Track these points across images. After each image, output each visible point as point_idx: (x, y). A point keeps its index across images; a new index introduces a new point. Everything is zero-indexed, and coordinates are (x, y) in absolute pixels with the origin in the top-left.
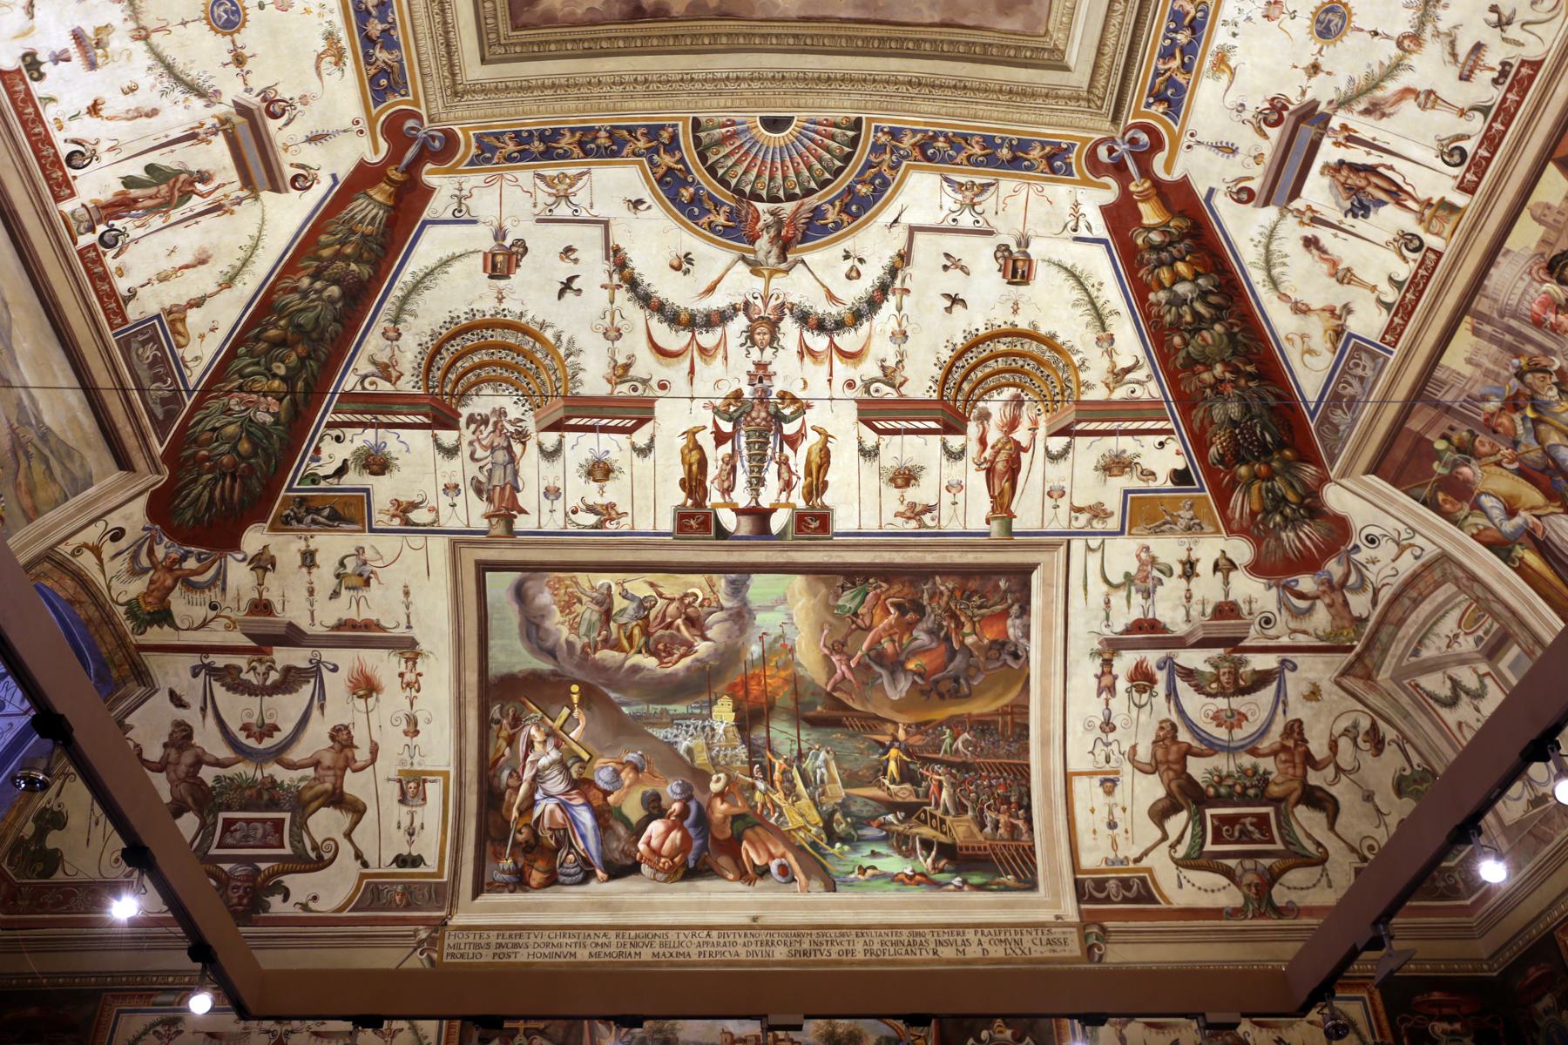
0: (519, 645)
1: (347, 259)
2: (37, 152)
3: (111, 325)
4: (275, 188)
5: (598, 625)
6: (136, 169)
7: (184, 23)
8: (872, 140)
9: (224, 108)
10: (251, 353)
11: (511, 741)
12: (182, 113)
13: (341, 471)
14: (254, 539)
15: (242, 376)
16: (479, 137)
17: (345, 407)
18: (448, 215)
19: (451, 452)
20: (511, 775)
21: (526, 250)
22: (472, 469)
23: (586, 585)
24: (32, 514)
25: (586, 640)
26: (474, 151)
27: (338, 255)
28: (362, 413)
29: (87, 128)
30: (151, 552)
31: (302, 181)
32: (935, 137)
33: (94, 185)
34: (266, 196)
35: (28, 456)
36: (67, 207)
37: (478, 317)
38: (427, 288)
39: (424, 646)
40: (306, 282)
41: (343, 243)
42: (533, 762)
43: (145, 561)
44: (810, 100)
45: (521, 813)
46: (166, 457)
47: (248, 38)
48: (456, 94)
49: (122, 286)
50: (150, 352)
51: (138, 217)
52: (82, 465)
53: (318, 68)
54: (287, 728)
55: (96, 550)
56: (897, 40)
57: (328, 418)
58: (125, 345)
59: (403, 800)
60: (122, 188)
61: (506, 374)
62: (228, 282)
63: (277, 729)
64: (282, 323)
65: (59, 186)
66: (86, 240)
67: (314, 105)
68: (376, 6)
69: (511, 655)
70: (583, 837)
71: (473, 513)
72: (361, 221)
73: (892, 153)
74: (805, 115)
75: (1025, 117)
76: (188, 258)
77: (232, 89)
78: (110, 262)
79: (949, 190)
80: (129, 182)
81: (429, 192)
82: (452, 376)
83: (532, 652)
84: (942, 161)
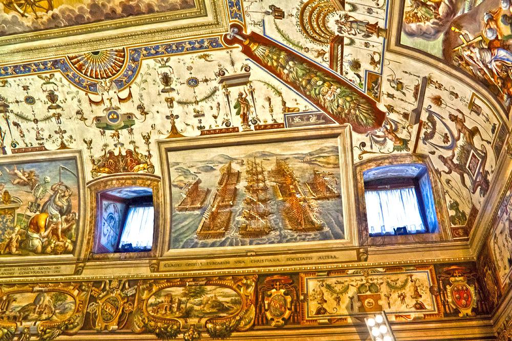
0: (432, 43)
1: (278, 59)
2: (223, 133)
3: (282, 128)
4: (249, 76)
5: (427, 9)
6: (234, 111)
7: (195, 92)
9: (220, 87)
10: (310, 91)
11: (467, 64)
12: (220, 97)
13: (359, 76)
14: (381, 107)
15: (319, 94)
16: (232, 18)
17: (335, 68)
18: (262, 28)
19: (352, 42)
20: (480, 72)
21: (273, 5)
22: (359, 36)
23: (409, 9)
24: (337, 166)
25: (433, 16)
26: (237, 20)
27: (277, 61)
28: (337, 64)
29: (220, 120)
30: (379, 137)
31: (247, 69)
33: (236, 121)
34: (250, 79)
35: (316, 161)
36: (241, 129)
37: (299, 23)
38: (288, 37)
39: (427, 75)
40: (286, 71)
41: (272, 59)
42: (477, 60)
43: (381, 139)
45: (493, 78)
46: (341, 123)
47: (200, 77)
48: (218, 24)
49: (270, 122)
50: (297, 120)
51: (249, 113)
52: (328, 148)
53: (210, 61)
54: (447, 131)
55: (365, 152)
57: (339, 74)
58: (290, 126)
59: (479, 115)
60: (239, 116)
61: (321, 18)
62: (280, 94)
63: (446, 134)
64: (300, 80)
65: (234, 130)
66: (252, 127)
67: (222, 63)
68: (190, 45)
69: (436, 46)
70: (508, 60)
71: (377, 41)
72: (264, 53)
76: (267, 103)
77: (215, 84)
78: (262, 123)
80: (238, 113)
81: (253, 33)
82: (323, 35)
83: (435, 39)
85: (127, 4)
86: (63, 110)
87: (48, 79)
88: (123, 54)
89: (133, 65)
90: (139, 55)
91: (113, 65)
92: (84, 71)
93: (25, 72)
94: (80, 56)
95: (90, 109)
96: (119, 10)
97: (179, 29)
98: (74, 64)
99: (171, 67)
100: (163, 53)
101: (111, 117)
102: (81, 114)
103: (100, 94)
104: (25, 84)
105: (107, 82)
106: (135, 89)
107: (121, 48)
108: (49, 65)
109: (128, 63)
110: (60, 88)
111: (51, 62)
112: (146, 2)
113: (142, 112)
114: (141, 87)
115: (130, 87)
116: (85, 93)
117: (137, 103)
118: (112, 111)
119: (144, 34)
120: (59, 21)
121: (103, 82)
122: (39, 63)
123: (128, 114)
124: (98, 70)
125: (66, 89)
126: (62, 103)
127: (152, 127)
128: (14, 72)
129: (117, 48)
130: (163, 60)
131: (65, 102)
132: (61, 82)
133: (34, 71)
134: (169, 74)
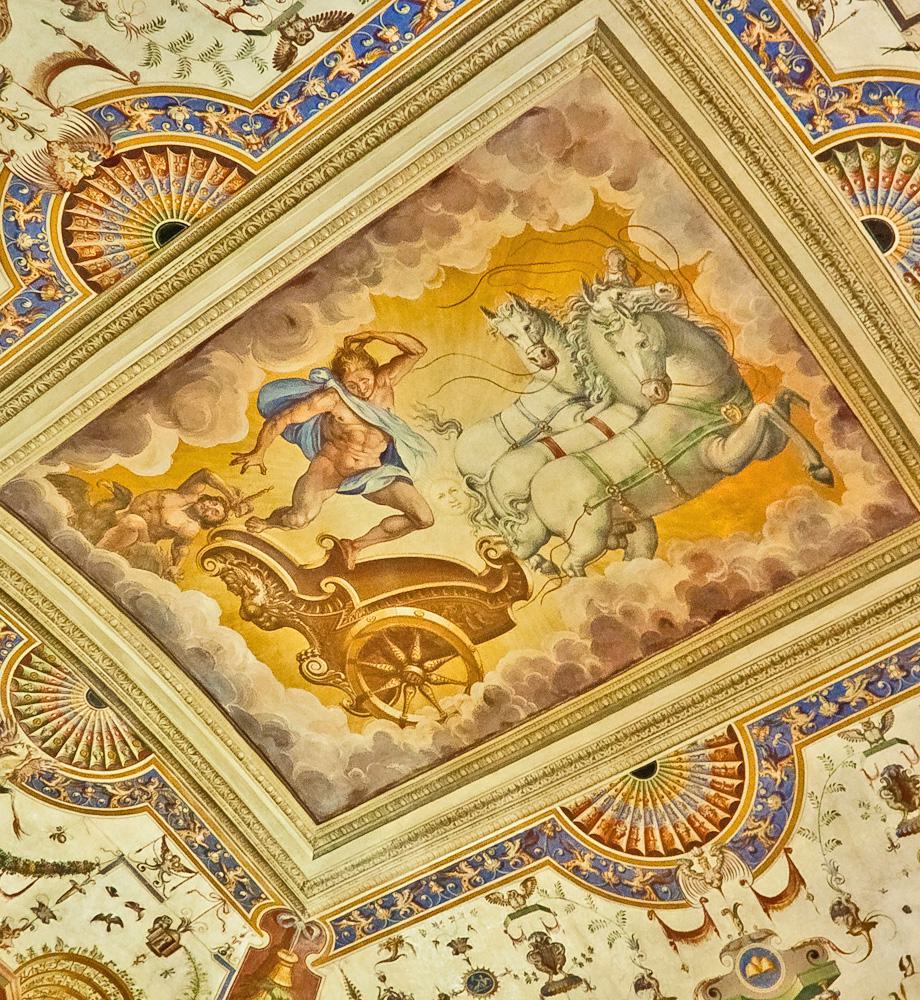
8: (832, 133)
32: (780, 78)
44: (832, 218)
56: (708, 186)
73: (831, 104)
74: (853, 213)
75: (683, 16)
79: (827, 21)
84: (799, 50)
85: (701, 585)
86: (589, 988)
87: (520, 900)
88: (731, 747)
89: (777, 775)
90: (786, 733)
91: (713, 792)
92: (623, 843)
93: (447, 895)
94: (600, 796)
95: (676, 961)
96: (680, 613)
97: (892, 604)
98: (585, 828)
99: (905, 742)
100: (863, 703)
101: (751, 970)
102: (649, 986)
103: (695, 901)
104: (456, 933)
105: (707, 855)
106: (805, 852)
107: (721, 730)
108: (512, 853)
109: (758, 771)
110: (563, 919)
111: (518, 842)
112: (758, 558)
113: (854, 925)
114: (824, 841)
115: (788, 851)
116: (645, 912)
117: (827, 899)
118: (750, 949)
119: (782, 659)
120: (510, 705)
121: (695, 860)
122: (479, 854)
123: (805, 944)
124: (668, 823)
125: (582, 917)
126: (581, 965)
127: (902, 967)
128: (415, 907)
129: (709, 735)
130: (869, 725)
131: (590, 960)
132: (563, 897)
133: (475, 884)
134: (906, 766)
